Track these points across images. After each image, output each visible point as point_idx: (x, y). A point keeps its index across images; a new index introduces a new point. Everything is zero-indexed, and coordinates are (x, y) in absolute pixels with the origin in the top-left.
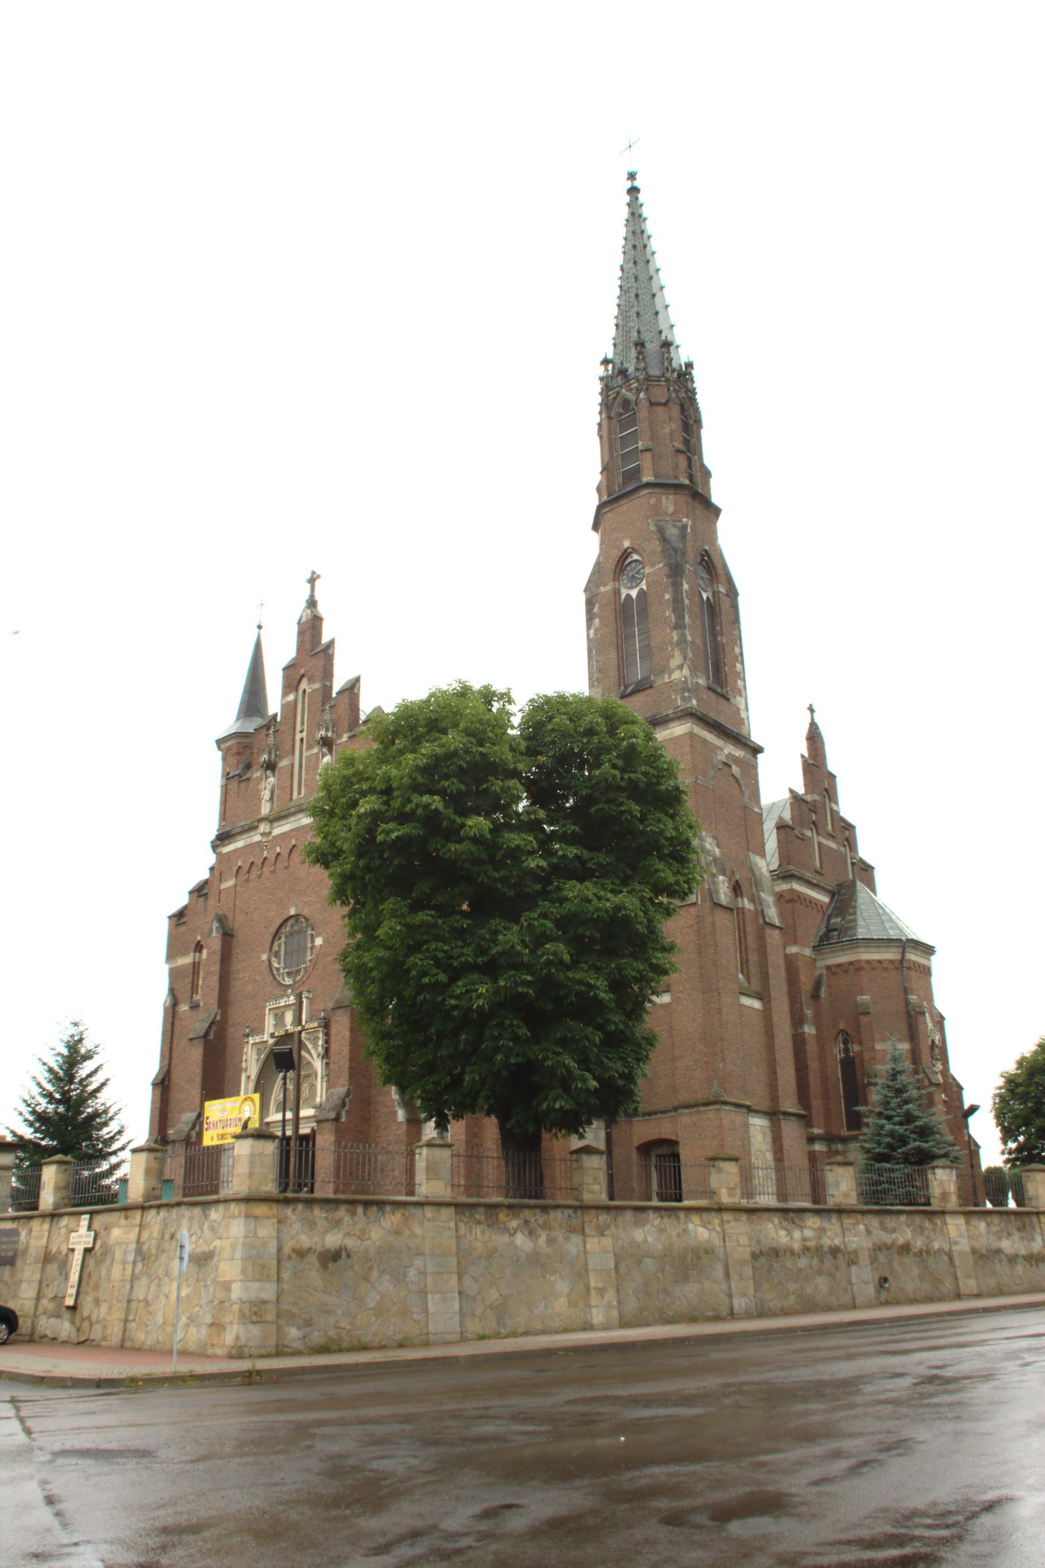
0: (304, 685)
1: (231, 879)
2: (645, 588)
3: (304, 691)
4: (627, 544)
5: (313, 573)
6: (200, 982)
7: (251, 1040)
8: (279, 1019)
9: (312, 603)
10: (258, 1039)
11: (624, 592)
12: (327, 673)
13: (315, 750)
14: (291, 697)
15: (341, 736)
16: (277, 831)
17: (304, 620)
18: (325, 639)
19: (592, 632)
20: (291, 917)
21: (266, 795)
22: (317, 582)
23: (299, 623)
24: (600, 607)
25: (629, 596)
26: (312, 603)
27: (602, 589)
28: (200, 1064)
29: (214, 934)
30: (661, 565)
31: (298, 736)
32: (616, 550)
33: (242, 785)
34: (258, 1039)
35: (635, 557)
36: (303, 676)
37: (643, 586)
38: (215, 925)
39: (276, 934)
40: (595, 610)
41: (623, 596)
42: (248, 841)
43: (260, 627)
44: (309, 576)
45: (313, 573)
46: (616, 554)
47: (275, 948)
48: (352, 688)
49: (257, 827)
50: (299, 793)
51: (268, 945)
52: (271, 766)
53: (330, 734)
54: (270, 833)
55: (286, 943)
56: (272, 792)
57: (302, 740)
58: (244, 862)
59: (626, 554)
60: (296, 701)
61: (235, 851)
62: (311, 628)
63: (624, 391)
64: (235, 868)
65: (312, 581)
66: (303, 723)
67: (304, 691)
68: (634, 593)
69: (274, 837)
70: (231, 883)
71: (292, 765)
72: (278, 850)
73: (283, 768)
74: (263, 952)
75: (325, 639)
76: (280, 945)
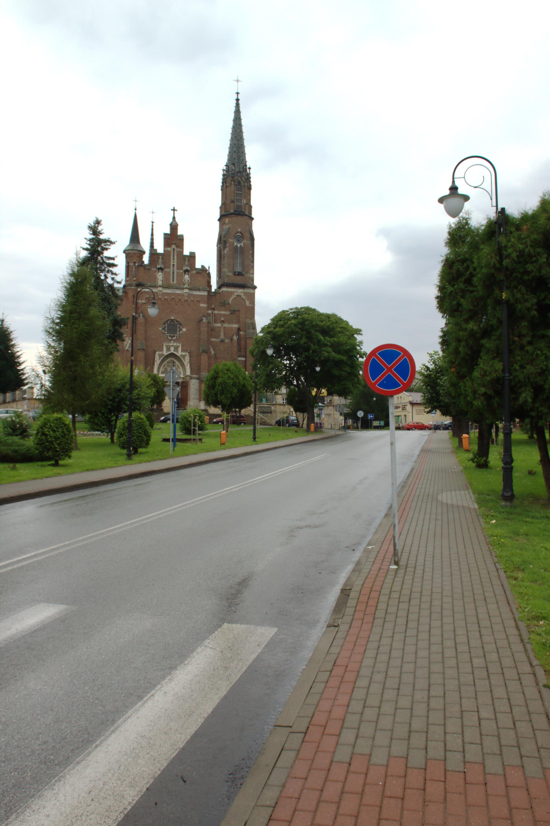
4: (239, 230)
8: (168, 349)
9: (174, 218)
10: (161, 353)
11: (235, 244)
13: (181, 271)
14: (169, 249)
25: (237, 245)
26: (174, 218)
29: (141, 317)
31: (172, 263)
34: (161, 353)
48: (192, 256)
50: (173, 281)
52: (161, 269)
57: (174, 265)
66: (174, 259)
68: (239, 245)
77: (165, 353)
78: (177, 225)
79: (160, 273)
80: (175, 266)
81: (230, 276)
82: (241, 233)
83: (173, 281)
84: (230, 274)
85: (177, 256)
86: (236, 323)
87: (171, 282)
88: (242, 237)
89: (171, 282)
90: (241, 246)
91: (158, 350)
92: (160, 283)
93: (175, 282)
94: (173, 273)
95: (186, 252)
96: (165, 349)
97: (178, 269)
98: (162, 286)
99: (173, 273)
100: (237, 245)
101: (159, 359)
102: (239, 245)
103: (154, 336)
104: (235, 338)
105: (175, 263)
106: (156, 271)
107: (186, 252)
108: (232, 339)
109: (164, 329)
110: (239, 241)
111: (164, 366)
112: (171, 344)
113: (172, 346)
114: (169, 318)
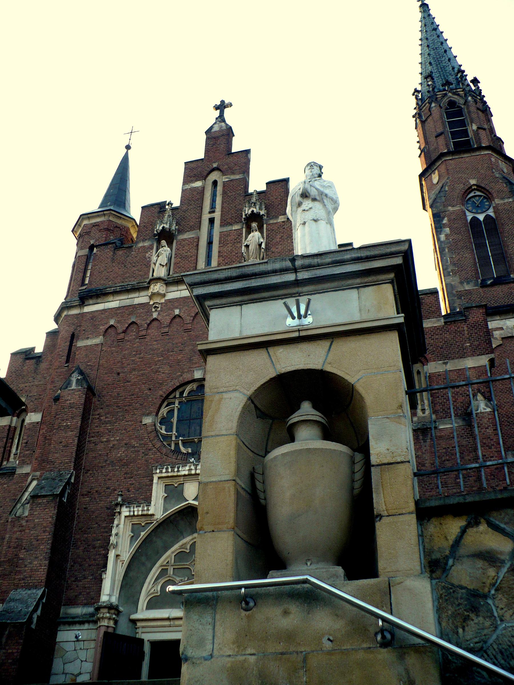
0: (214, 176)
1: (97, 336)
2: (492, 214)
3: (215, 183)
4: (473, 182)
5: (223, 102)
6: (14, 450)
7: (125, 512)
8: (174, 492)
12: (245, 170)
13: (236, 227)
14: (198, 184)
15: (277, 217)
16: (170, 296)
17: (216, 128)
18: (237, 146)
19: (443, 237)
20: (194, 381)
21: (163, 259)
22: (226, 110)
23: (208, 132)
24: (449, 220)
25: (474, 219)
27: (450, 208)
28: (50, 528)
29: (74, 386)
30: (511, 200)
31: (206, 217)
32: (462, 186)
33: (120, 252)
34: (138, 511)
35: (478, 193)
36: (213, 170)
37: (491, 212)
38: (75, 377)
39: (167, 399)
40: (445, 222)
41: (469, 218)
42: (128, 302)
43: (128, 147)
44: (218, 103)
45: (223, 102)
46: (460, 187)
47: (164, 411)
49: (147, 288)
50: (208, 262)
51: (153, 409)
52: (167, 236)
53: (262, 213)
54: (164, 295)
55: (179, 410)
56: (170, 259)
57: (212, 221)
58: (118, 322)
59: (470, 189)
60: (203, 188)
61: (104, 311)
62: (219, 138)
63: (450, 94)
64: (103, 328)
65: (222, 107)
67: (215, 183)
68: (481, 217)
69: (170, 301)
70: (98, 340)
71: (198, 239)
72: (177, 312)
73: (184, 240)
74: (148, 415)
75: (237, 146)
76: (171, 411)
77: (158, 508)
78: (231, 128)
79: (165, 251)
80: (217, 222)
81: (469, 292)
82: (479, 188)
83: (208, 262)
84: (467, 287)
85: (224, 193)
86: (476, 352)
87: (201, 265)
88: (488, 196)
89: (201, 265)
90: (487, 217)
91: (128, 502)
92: (161, 272)
93: (214, 263)
94: (210, 243)
95: (257, 183)
96: (158, 492)
97: (223, 223)
98: (169, 282)
99: (210, 243)
100: (474, 219)
101: (133, 539)
102: (481, 217)
103: (120, 453)
104: (481, 406)
105: (217, 215)
106: (151, 248)
107: (257, 183)
108: (467, 415)
109: (165, 421)
110: (479, 208)
111: (164, 572)
112: (184, 471)
113: (189, 476)
114: (187, 377)
